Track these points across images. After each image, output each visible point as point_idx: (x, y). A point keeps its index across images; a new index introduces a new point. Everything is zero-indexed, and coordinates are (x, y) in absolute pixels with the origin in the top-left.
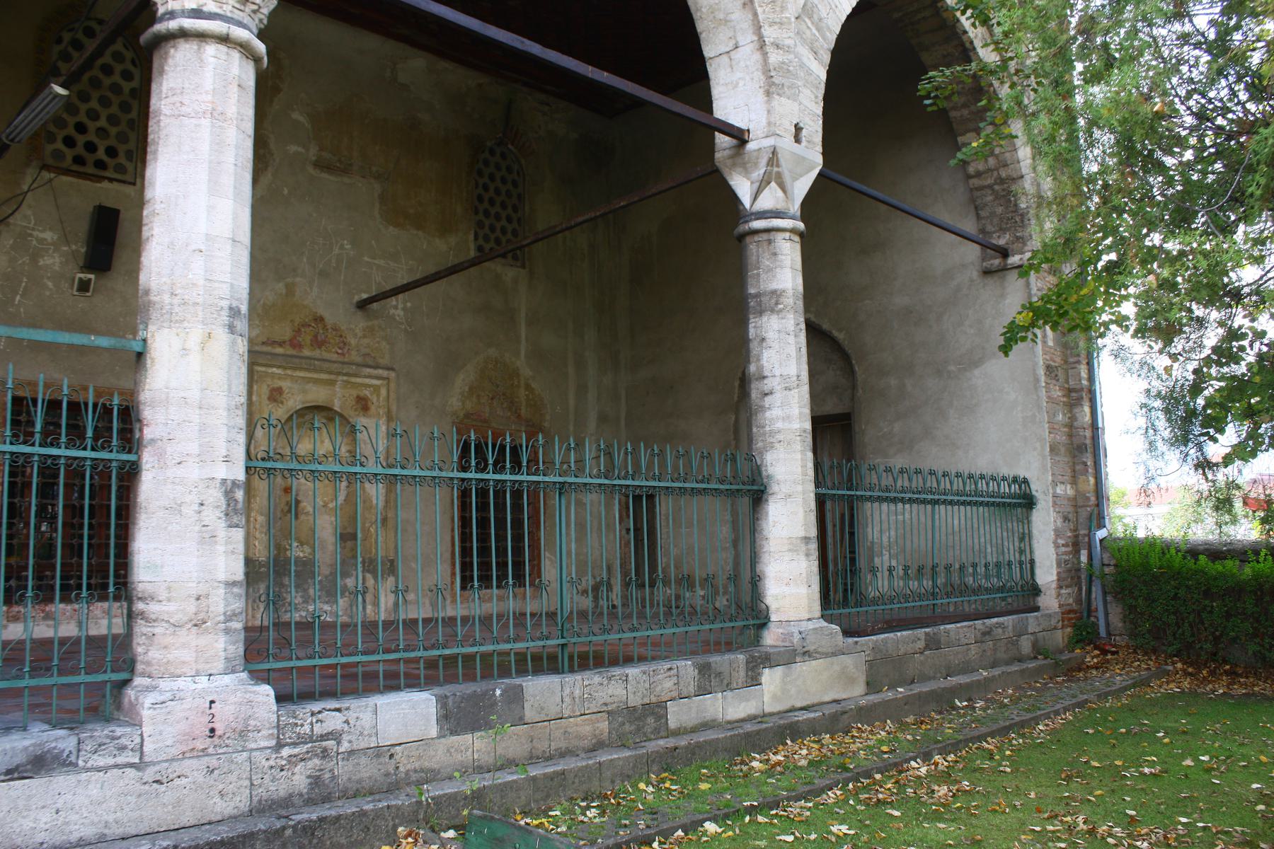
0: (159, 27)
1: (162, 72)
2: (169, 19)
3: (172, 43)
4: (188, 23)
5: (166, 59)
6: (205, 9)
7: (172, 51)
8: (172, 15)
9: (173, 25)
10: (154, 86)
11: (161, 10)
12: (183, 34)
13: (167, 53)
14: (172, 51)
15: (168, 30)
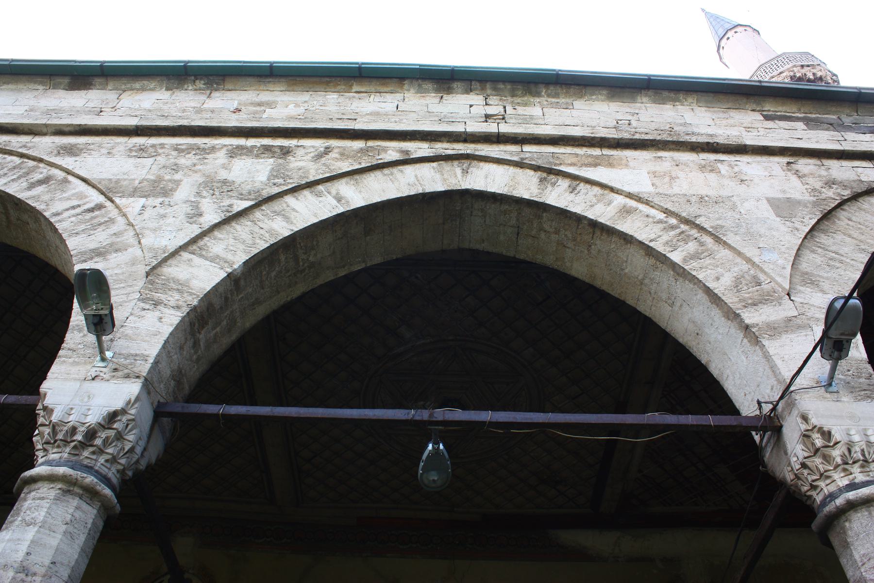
0: (830, 508)
1: (846, 545)
2: (830, 501)
3: (844, 518)
4: (851, 495)
5: (845, 533)
6: (856, 481)
7: (847, 524)
8: (832, 496)
9: (839, 501)
10: (843, 561)
11: (819, 499)
12: (852, 506)
13: (843, 528)
14: (847, 524)
15: (837, 507)
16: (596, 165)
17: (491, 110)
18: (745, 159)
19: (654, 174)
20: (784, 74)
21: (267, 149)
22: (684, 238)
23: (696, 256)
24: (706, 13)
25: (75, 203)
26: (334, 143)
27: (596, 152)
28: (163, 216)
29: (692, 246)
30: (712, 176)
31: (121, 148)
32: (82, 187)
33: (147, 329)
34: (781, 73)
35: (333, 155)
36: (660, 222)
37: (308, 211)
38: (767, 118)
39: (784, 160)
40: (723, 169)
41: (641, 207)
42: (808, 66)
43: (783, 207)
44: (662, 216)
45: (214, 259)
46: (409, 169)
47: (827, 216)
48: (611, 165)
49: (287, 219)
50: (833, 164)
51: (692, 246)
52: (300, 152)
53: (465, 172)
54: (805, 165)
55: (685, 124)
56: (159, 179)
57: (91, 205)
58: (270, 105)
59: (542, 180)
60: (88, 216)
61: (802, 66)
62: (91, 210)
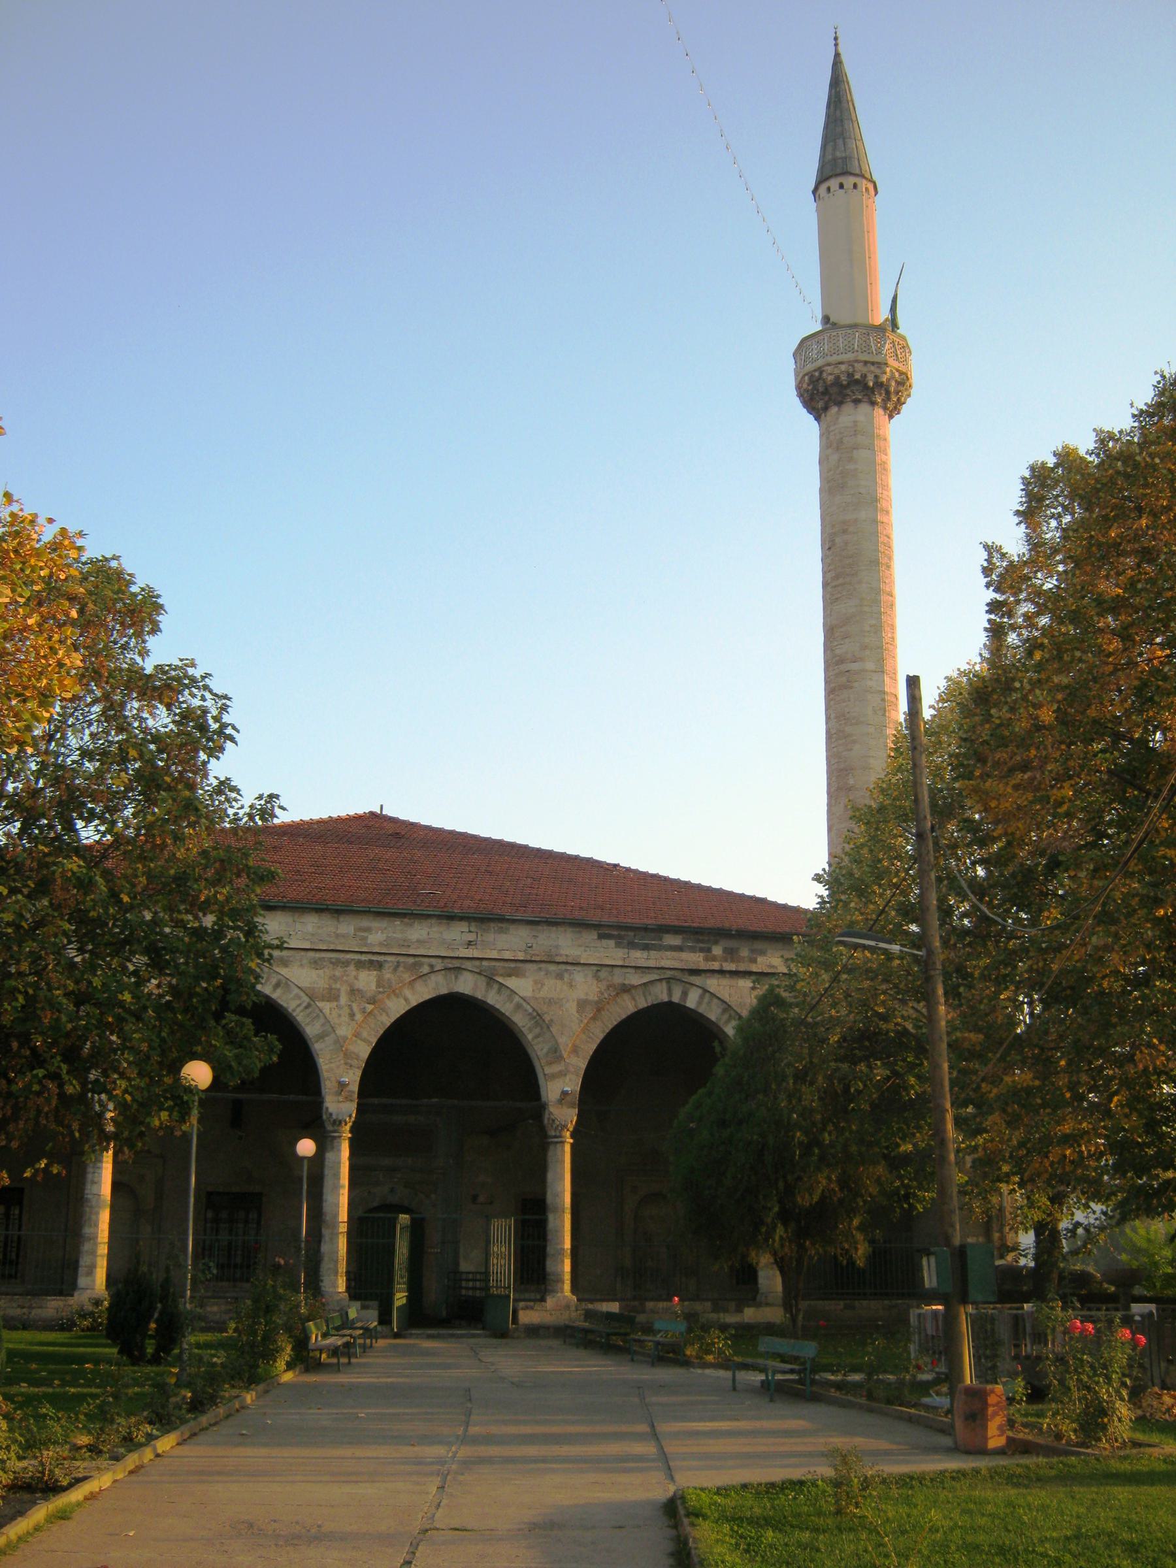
16: (510, 976)
17: (472, 937)
18: (578, 968)
19: (536, 982)
20: (843, 367)
21: (371, 962)
22: (537, 1024)
23: (537, 1037)
24: (837, 55)
25: (298, 1002)
26: (401, 959)
27: (513, 965)
28: (340, 1016)
29: (537, 1030)
30: (559, 982)
31: (305, 961)
32: (296, 991)
33: (352, 1078)
34: (840, 363)
35: (401, 969)
36: (530, 1014)
37: (397, 1008)
38: (601, 937)
39: (595, 968)
40: (566, 976)
41: (524, 1004)
42: (873, 363)
43: (582, 1004)
44: (530, 1010)
45: (364, 1040)
46: (433, 977)
47: (599, 1010)
48: (517, 976)
49: (387, 1015)
50: (617, 971)
51: (537, 1030)
52: (387, 965)
53: (456, 977)
54: (603, 974)
55: (557, 947)
56: (331, 989)
57: (305, 1004)
58: (368, 930)
59: (488, 984)
60: (308, 1011)
61: (866, 363)
62: (306, 1008)
